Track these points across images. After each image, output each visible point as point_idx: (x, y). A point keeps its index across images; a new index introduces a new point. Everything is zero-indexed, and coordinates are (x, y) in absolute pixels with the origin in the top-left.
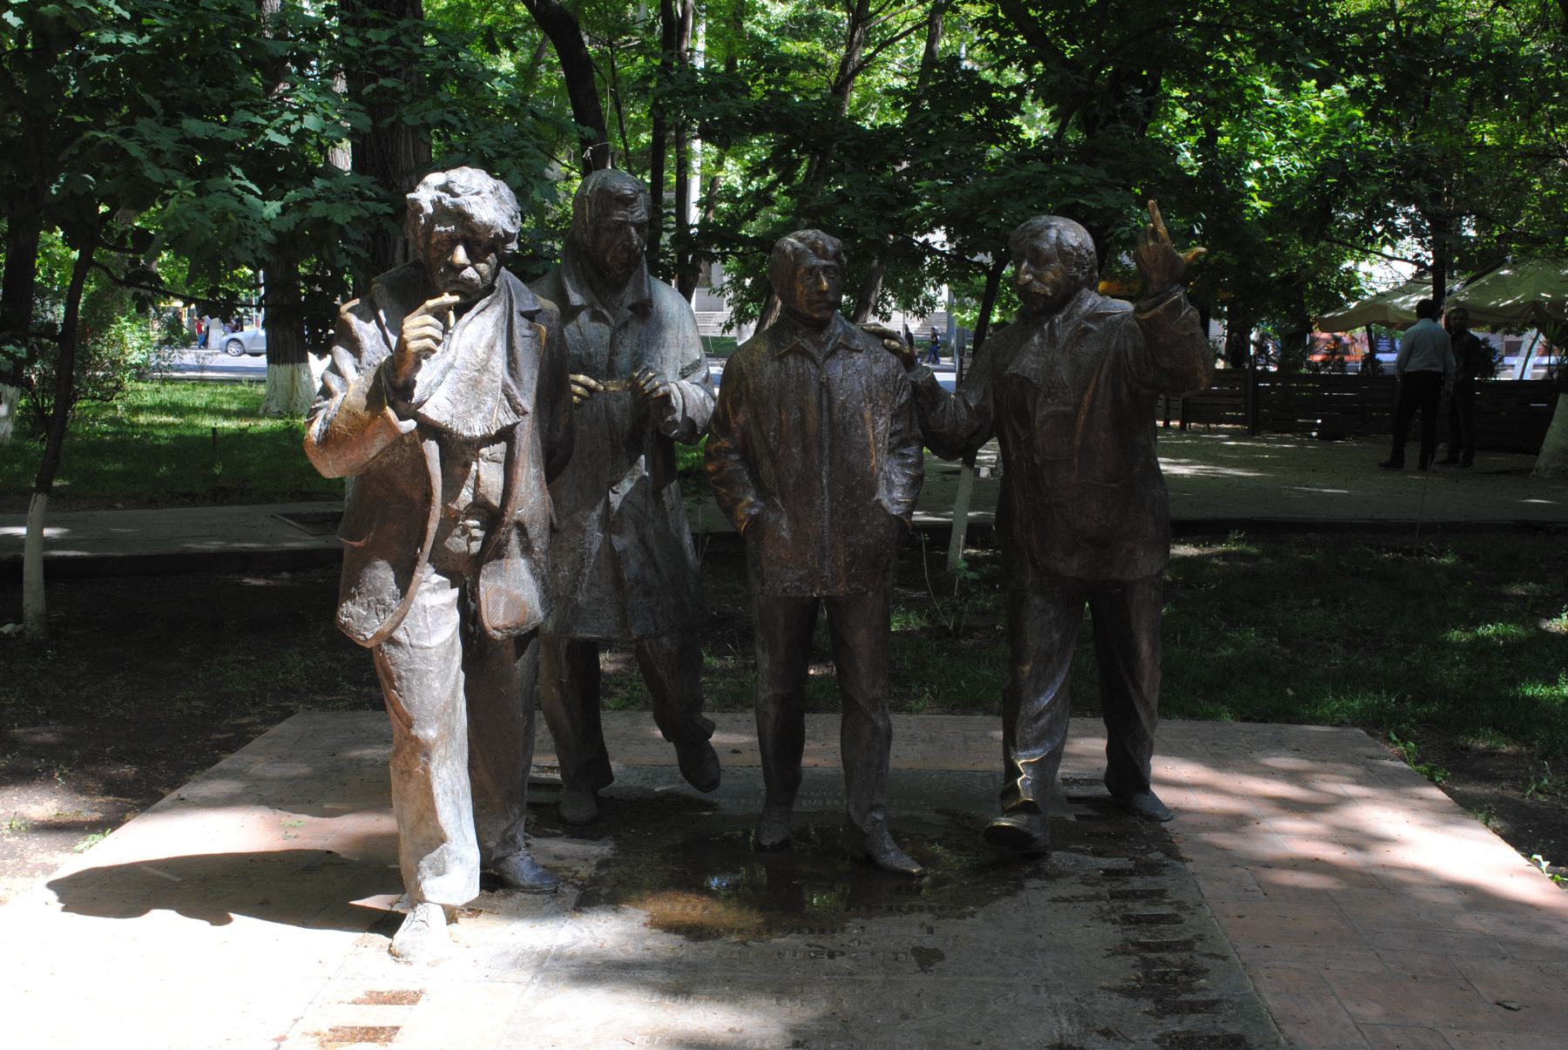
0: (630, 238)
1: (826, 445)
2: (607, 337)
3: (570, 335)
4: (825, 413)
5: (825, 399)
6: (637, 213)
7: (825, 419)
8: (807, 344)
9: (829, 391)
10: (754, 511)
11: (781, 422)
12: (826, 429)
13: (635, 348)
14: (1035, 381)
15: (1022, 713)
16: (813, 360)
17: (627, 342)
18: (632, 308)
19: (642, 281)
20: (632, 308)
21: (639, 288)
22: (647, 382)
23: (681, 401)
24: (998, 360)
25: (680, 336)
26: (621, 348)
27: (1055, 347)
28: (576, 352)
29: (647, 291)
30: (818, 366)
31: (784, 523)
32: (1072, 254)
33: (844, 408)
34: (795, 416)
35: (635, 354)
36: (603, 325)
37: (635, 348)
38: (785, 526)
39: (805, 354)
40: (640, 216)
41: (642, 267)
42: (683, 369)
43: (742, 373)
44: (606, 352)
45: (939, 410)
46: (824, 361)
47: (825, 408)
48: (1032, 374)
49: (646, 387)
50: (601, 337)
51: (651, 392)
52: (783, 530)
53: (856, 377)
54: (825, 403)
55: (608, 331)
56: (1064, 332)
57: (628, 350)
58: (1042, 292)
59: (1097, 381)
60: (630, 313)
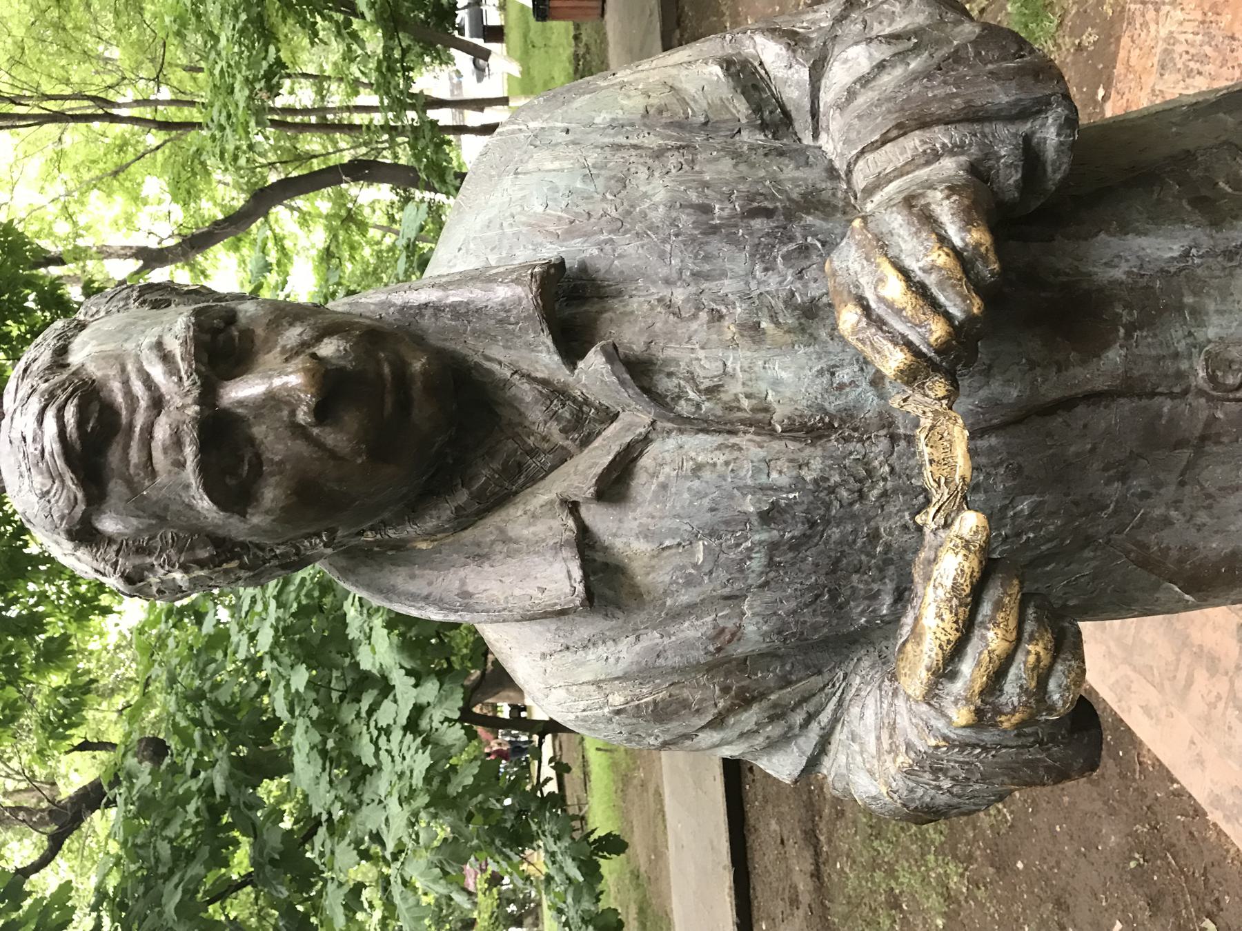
0: (272, 401)
2: (699, 446)
3: (690, 582)
6: (157, 372)
13: (729, 329)
17: (707, 367)
18: (571, 347)
19: (461, 312)
20: (571, 347)
21: (502, 318)
22: (935, 306)
23: (940, 136)
25: (653, 141)
26: (734, 388)
28: (757, 563)
29: (502, 293)
35: (752, 330)
36: (646, 461)
37: (729, 329)
40: (166, 358)
41: (404, 309)
42: (763, 127)
44: (751, 447)
49: (957, 312)
50: (698, 469)
51: (979, 287)
55: (671, 443)
57: (738, 360)
60: (594, 361)
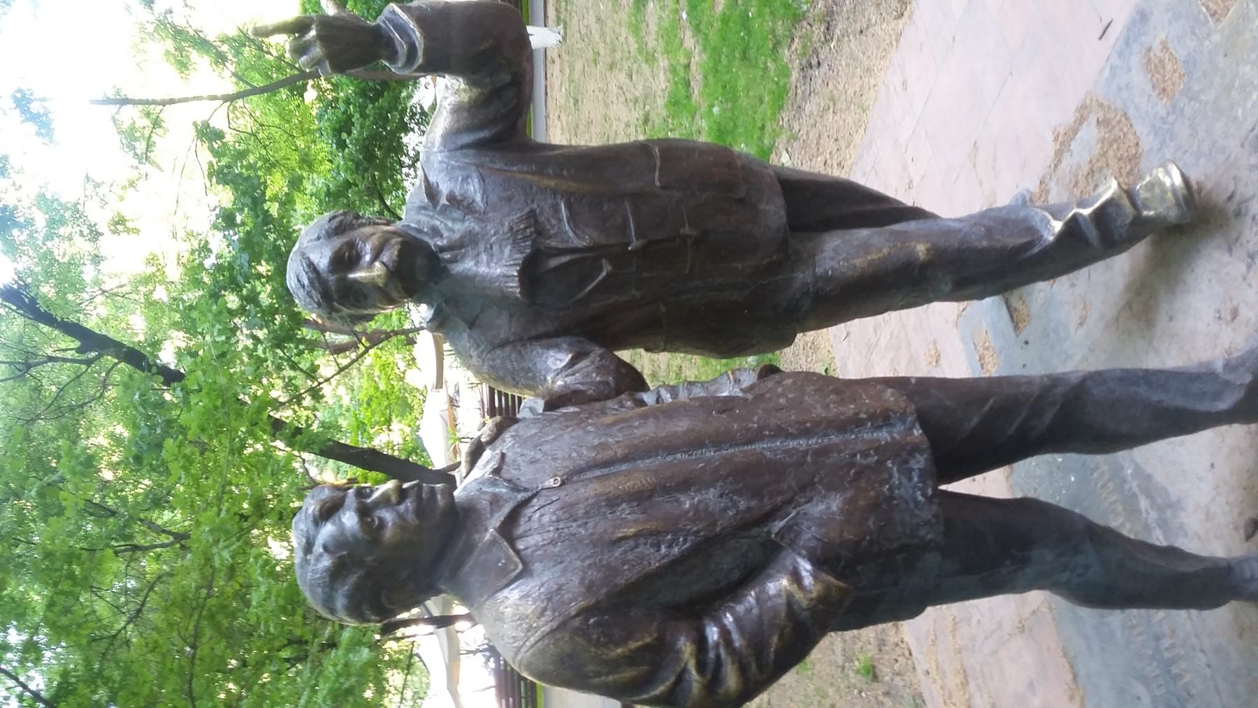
1: (669, 458)
4: (613, 469)
5: (589, 475)
7: (624, 467)
8: (495, 522)
9: (580, 471)
10: (805, 567)
11: (636, 535)
12: (641, 464)
14: (528, 251)
15: (985, 243)
16: (525, 503)
24: (502, 336)
27: (477, 234)
30: (534, 496)
31: (817, 509)
32: (341, 221)
33: (603, 446)
34: (624, 510)
38: (821, 507)
39: (513, 518)
45: (581, 387)
46: (526, 490)
47: (606, 471)
48: (519, 256)
52: (828, 508)
53: (546, 448)
54: (598, 473)
56: (452, 228)
58: (398, 247)
59: (519, 172)
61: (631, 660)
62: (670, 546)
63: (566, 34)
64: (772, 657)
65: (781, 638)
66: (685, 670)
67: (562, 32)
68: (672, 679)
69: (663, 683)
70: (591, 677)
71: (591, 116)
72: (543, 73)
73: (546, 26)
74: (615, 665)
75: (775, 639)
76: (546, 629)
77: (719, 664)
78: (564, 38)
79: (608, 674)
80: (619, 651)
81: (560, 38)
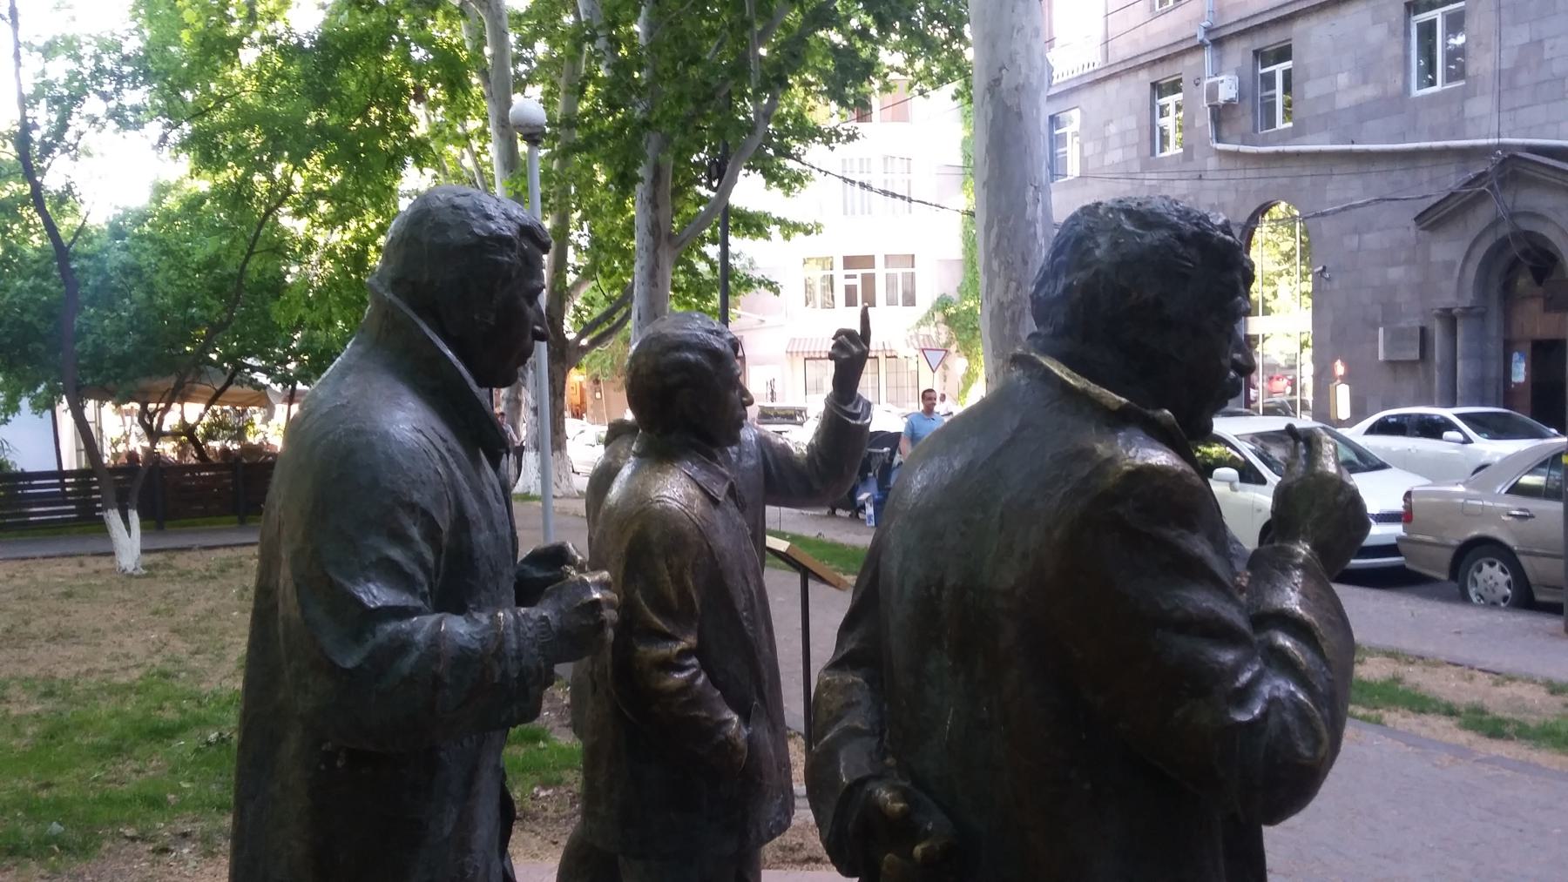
43: (700, 530)
61: (683, 593)
62: (746, 618)
63: (138, 577)
64: (692, 714)
65: (706, 718)
66: (676, 640)
67: (136, 573)
68: (669, 631)
69: (665, 623)
70: (666, 561)
71: (77, 616)
72: (51, 553)
73: (144, 551)
74: (679, 580)
75: (704, 714)
76: (698, 522)
77: (682, 669)
78: (131, 576)
79: (671, 575)
80: (691, 583)
81: (130, 570)
